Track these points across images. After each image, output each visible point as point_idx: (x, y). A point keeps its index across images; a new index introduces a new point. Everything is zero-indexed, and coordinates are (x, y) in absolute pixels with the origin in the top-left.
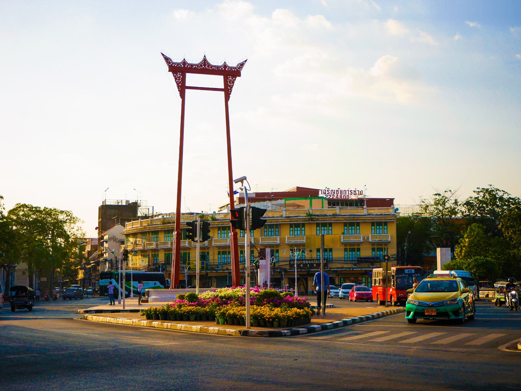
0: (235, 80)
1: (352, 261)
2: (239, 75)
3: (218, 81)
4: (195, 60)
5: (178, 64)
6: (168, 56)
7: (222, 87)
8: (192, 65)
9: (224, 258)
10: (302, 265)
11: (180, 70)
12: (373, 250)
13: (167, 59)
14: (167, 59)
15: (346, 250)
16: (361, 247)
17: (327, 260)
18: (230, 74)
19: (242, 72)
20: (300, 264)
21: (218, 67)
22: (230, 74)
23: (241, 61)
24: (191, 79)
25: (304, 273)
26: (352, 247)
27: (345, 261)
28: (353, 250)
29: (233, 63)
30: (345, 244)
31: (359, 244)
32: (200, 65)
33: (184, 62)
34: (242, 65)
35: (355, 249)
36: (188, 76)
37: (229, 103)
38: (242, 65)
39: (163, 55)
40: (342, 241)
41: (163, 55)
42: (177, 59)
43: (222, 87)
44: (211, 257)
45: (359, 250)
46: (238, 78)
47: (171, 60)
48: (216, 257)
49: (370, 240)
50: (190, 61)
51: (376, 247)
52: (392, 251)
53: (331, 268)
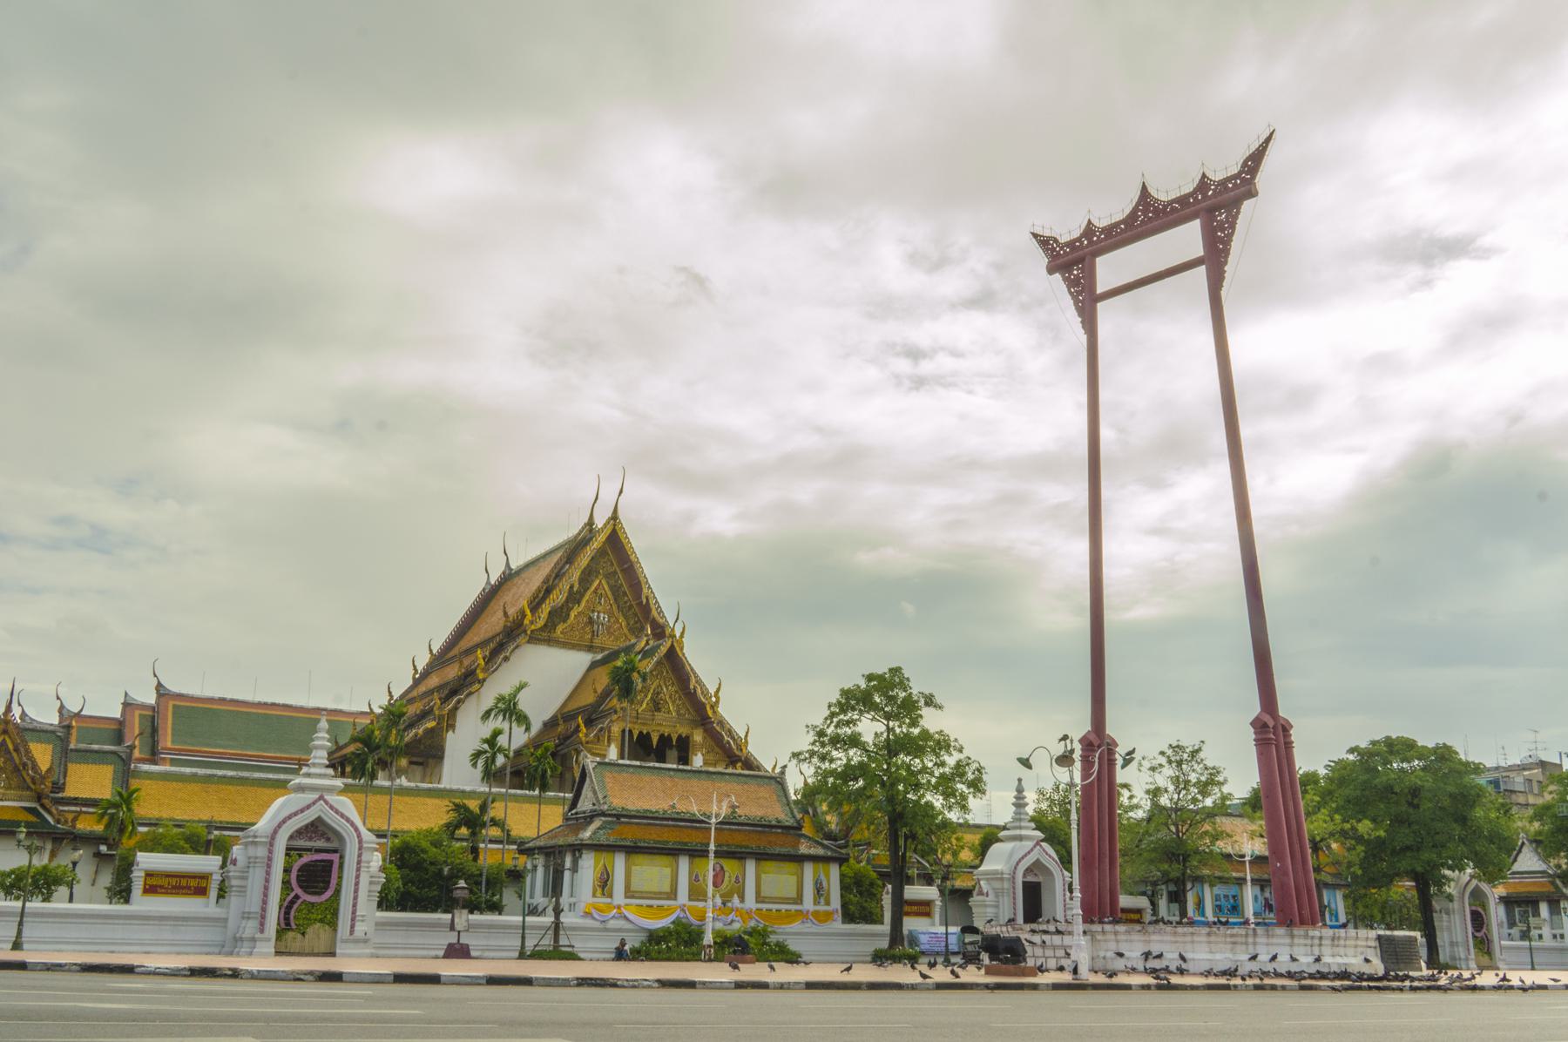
2: (1252, 194)
4: (1113, 209)
5: (1071, 244)
6: (1047, 233)
7: (1201, 253)
8: (1109, 230)
11: (1073, 260)
13: (1044, 242)
14: (1044, 242)
18: (1217, 206)
19: (1261, 180)
21: (1182, 200)
24: (1109, 269)
29: (1224, 166)
32: (1133, 215)
33: (1089, 230)
37: (1223, 293)
39: (1035, 235)
41: (1035, 235)
42: (1067, 230)
43: (1201, 253)
46: (1247, 205)
47: (1056, 240)
50: (1102, 222)
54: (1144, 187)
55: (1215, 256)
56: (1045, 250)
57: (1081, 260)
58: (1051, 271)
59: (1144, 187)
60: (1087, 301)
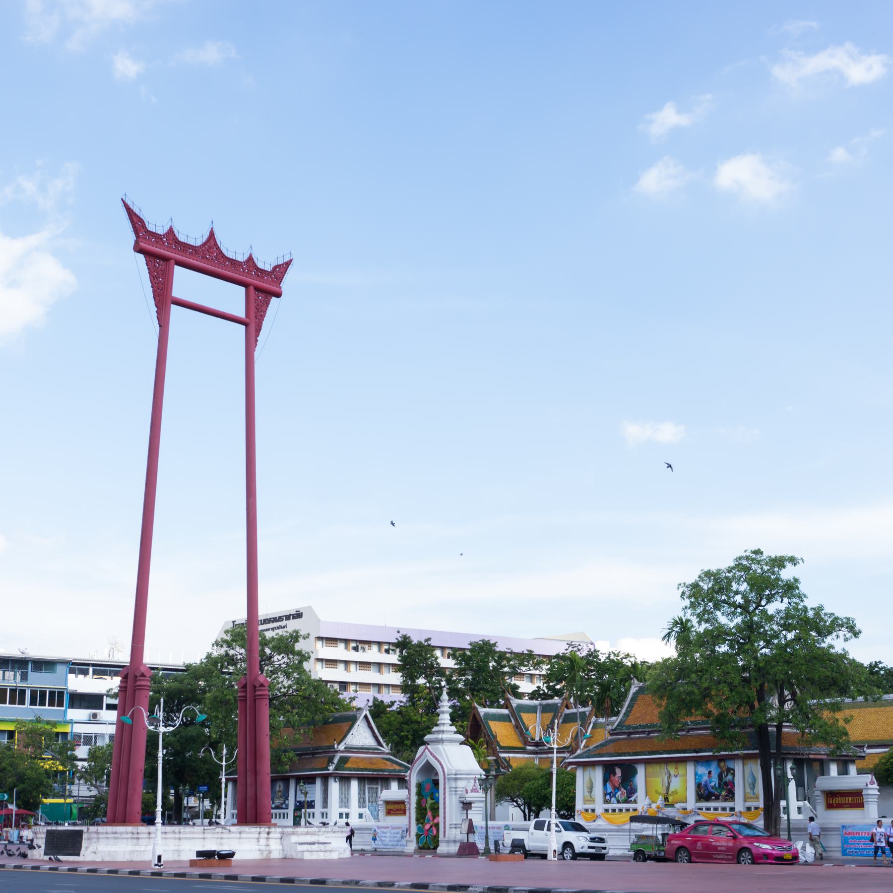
0: (267, 304)
2: (278, 295)
3: (233, 299)
4: (192, 234)
6: (137, 212)
8: (185, 247)
11: (161, 254)
18: (261, 286)
22: (261, 286)
23: (281, 262)
29: (266, 262)
34: (281, 269)
36: (179, 273)
37: (256, 354)
38: (281, 269)
42: (157, 224)
43: (241, 313)
46: (274, 299)
54: (212, 234)
55: (252, 323)
56: (136, 232)
57: (166, 259)
58: (138, 249)
59: (212, 234)
60: (163, 298)
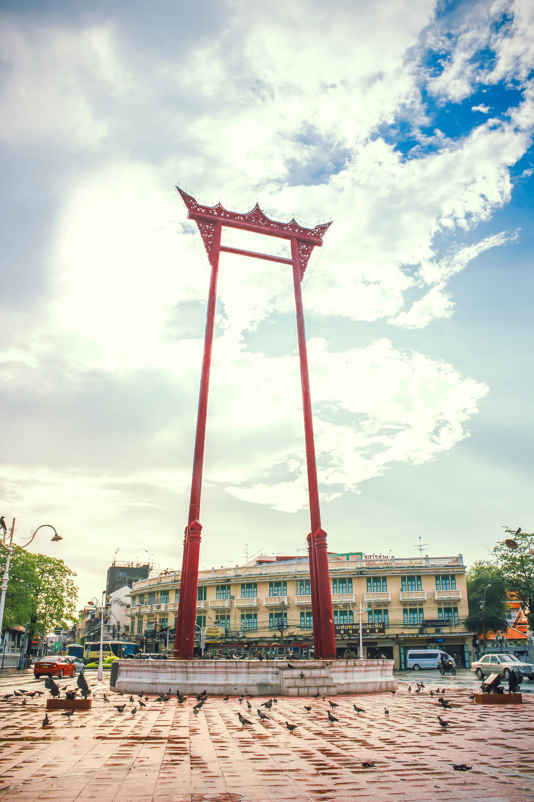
1: (414, 625)
9: (249, 623)
10: (351, 632)
12: (440, 610)
15: (405, 611)
16: (424, 607)
17: (383, 623)
20: (349, 630)
25: (354, 642)
26: (413, 608)
27: (405, 626)
28: (413, 611)
30: (404, 603)
31: (422, 603)
35: (416, 609)
40: (401, 599)
44: (232, 621)
45: (421, 611)
48: (238, 621)
49: (436, 598)
51: (443, 607)
52: (463, 612)
53: (389, 635)
